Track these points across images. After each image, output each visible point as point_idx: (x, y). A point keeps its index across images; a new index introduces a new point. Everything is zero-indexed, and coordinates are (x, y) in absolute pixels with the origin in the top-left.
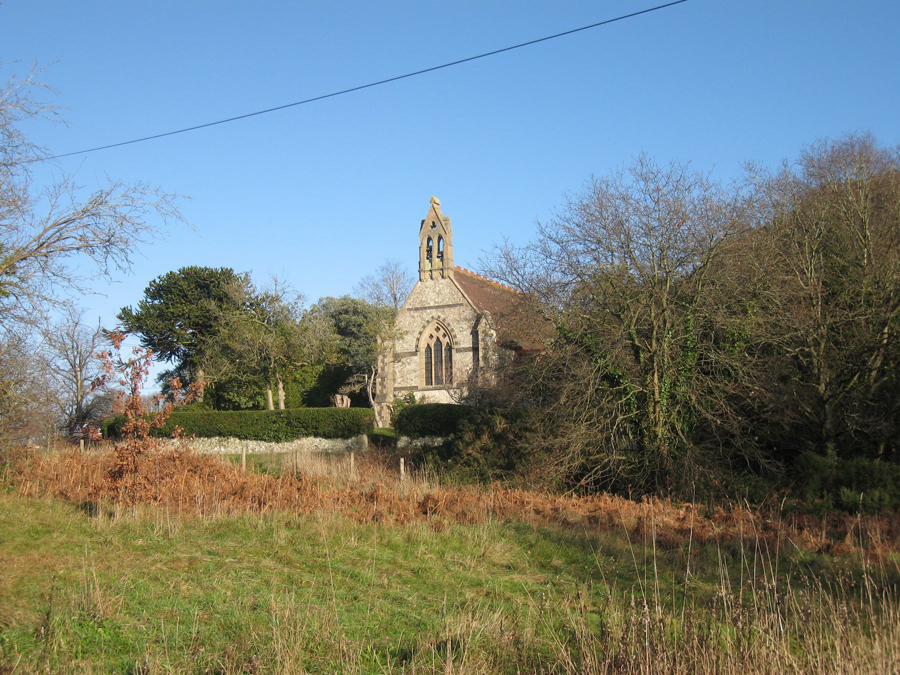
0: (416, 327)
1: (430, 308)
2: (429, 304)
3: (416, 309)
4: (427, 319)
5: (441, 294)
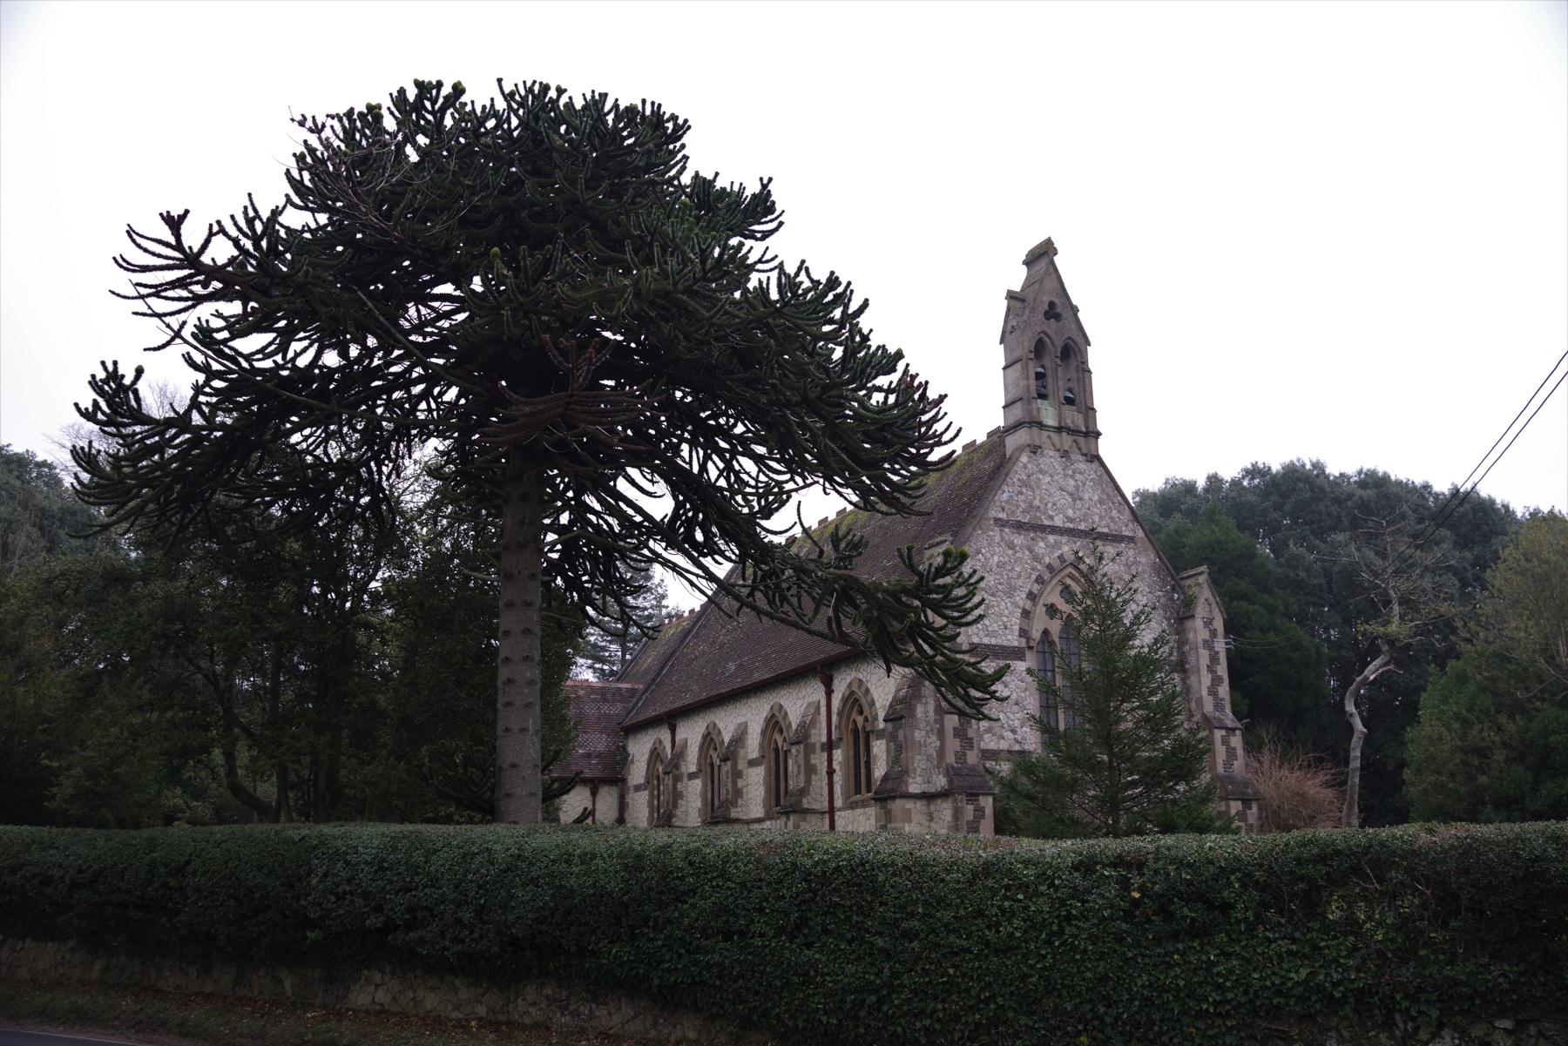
0: (1019, 576)
1: (1054, 530)
2: (1051, 518)
3: (1019, 526)
4: (1047, 560)
5: (1081, 499)
